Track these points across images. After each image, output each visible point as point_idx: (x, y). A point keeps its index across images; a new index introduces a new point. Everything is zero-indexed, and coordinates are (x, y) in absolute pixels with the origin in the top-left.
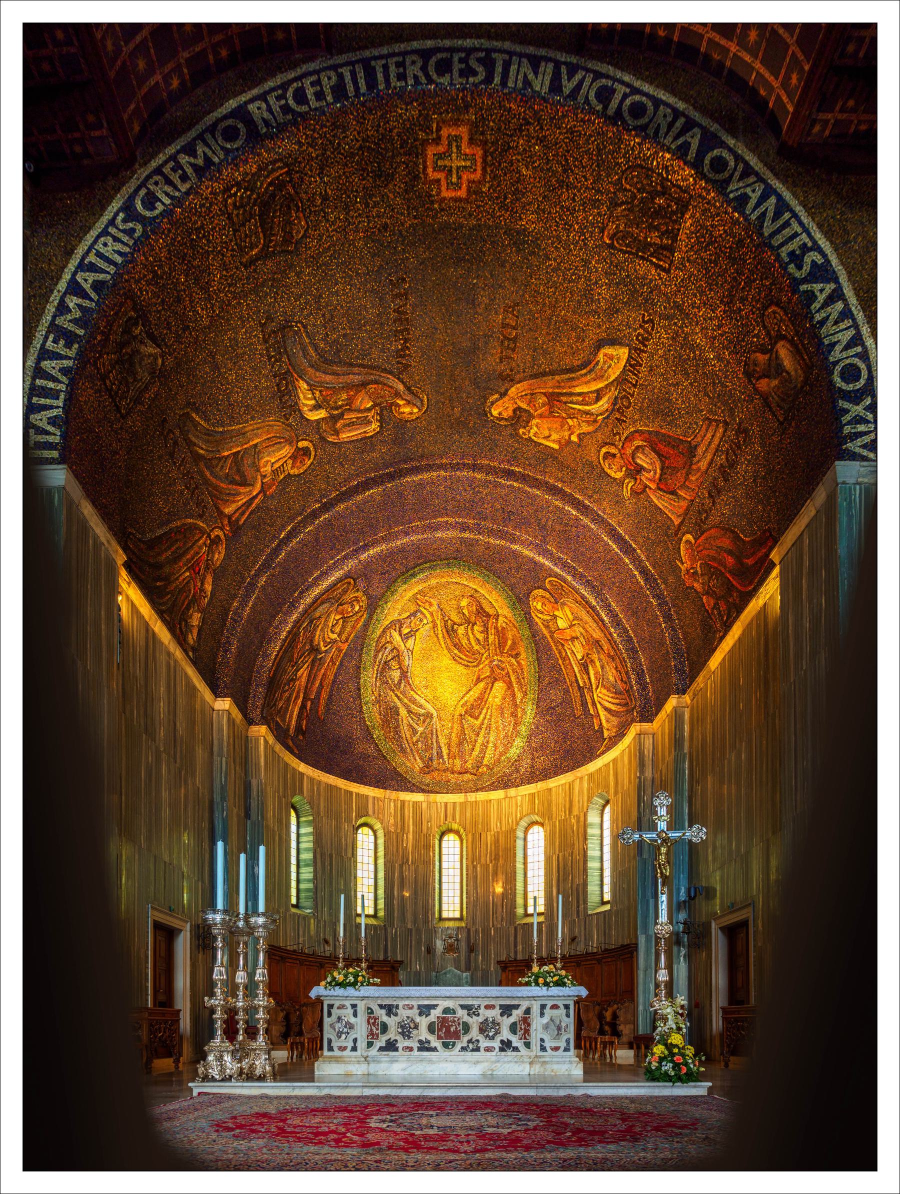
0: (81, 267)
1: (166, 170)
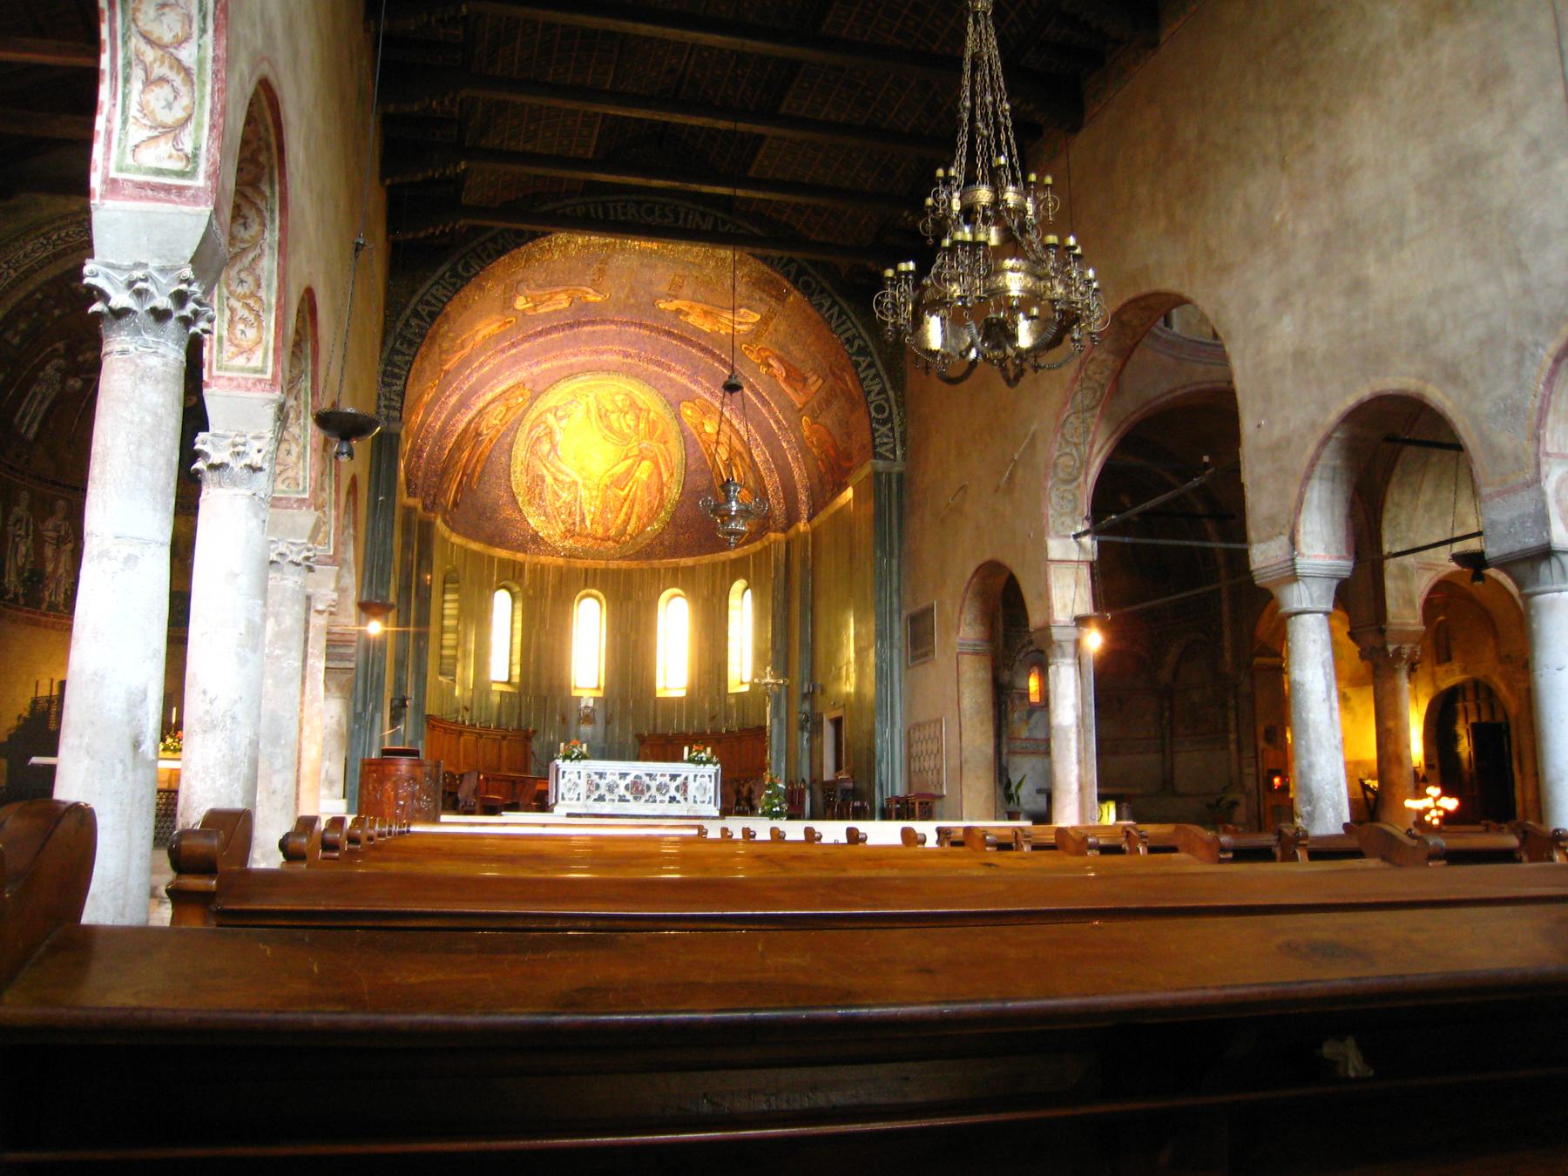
0: (421, 301)
1: (478, 250)
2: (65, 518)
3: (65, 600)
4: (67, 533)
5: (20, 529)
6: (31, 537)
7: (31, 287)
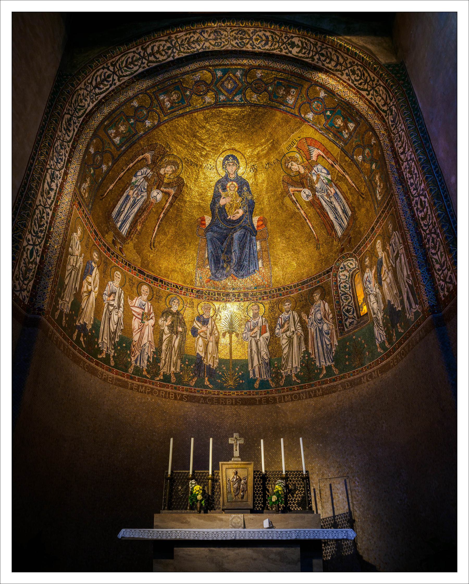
2: (149, 300)
3: (147, 366)
4: (149, 311)
5: (114, 300)
6: (122, 309)
7: (131, 94)
